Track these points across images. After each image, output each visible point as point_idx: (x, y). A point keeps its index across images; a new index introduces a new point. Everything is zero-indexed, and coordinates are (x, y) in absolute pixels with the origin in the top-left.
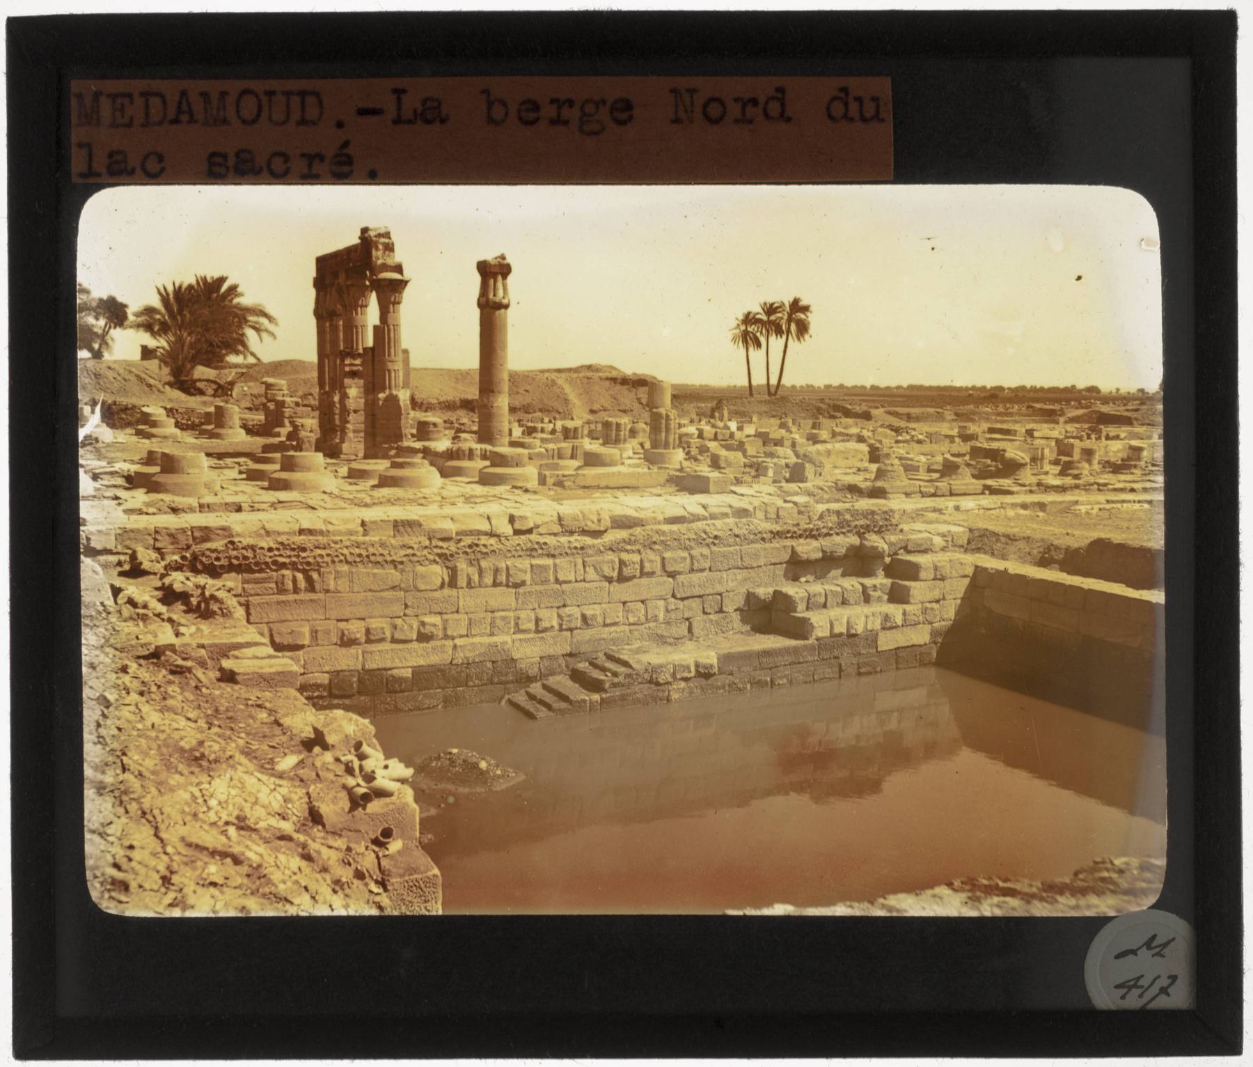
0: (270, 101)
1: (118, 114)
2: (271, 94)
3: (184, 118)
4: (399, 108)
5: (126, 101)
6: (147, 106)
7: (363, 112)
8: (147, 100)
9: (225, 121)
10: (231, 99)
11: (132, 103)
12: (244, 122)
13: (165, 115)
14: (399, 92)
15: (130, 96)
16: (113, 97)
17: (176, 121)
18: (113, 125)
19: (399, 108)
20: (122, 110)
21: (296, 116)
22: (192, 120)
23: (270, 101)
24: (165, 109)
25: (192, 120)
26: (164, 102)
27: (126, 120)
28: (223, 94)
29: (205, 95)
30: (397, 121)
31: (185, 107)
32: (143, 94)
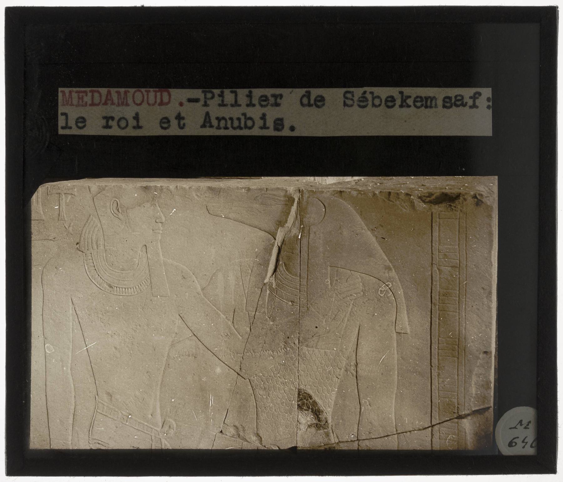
0: (148, 95)
1: (81, 101)
3: (109, 102)
5: (84, 94)
6: (93, 96)
7: (190, 100)
8: (93, 96)
9: (127, 105)
10: (130, 95)
11: (86, 96)
12: (137, 105)
13: (101, 100)
15: (85, 92)
23: (148, 95)
25: (113, 104)
26: (101, 96)
29: (118, 92)
32: (90, 91)
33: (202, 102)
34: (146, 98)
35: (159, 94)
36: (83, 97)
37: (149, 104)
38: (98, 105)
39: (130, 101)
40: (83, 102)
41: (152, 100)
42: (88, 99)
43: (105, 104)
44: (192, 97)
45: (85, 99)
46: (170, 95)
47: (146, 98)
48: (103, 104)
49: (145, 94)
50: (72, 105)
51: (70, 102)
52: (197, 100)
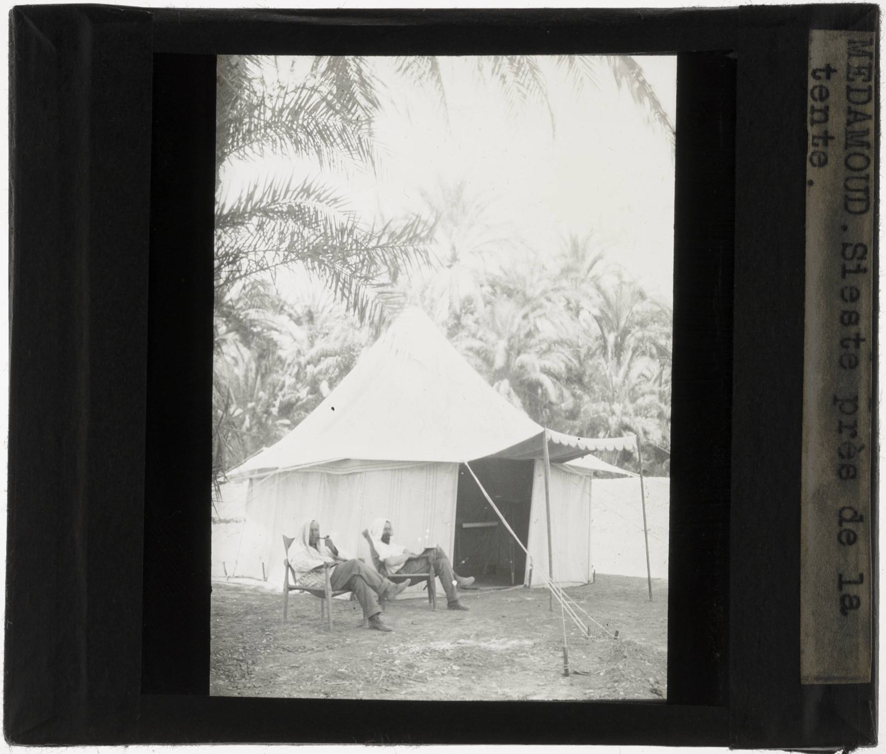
0: (861, 178)
3: (852, 117)
8: (865, 91)
11: (864, 81)
12: (846, 161)
20: (859, 73)
23: (861, 178)
31: (859, 117)
34: (855, 174)
36: (864, 74)
38: (848, 98)
39: (852, 150)
43: (849, 111)
45: (859, 79)
48: (849, 108)
49: (863, 174)
50: (850, 55)
51: (853, 52)
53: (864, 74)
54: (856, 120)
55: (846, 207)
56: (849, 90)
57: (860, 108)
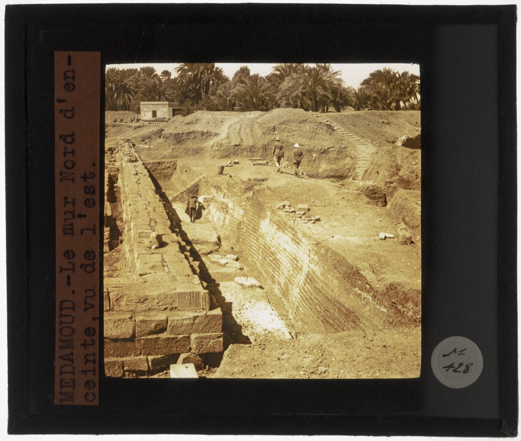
1: (70, 385)
2: (61, 323)
4: (69, 270)
6: (65, 373)
8: (65, 373)
11: (64, 379)
13: (69, 365)
14: (61, 270)
15: (61, 380)
16: (62, 387)
17: (72, 361)
18: (74, 387)
19: (69, 270)
21: (70, 312)
22: (72, 354)
24: (66, 365)
25: (72, 354)
26: (64, 365)
27: (71, 382)
28: (61, 341)
30: (73, 270)
31: (67, 357)
33: (70, 273)
35: (64, 312)
36: (65, 383)
37: (72, 323)
38: (74, 368)
40: (70, 383)
41: (69, 319)
42: (67, 377)
44: (65, 281)
46: (64, 301)
47: (66, 325)
49: (63, 325)
52: (69, 277)
53: (65, 383)
54: (69, 355)
55: (74, 304)
56: (73, 373)
57: (65, 362)
